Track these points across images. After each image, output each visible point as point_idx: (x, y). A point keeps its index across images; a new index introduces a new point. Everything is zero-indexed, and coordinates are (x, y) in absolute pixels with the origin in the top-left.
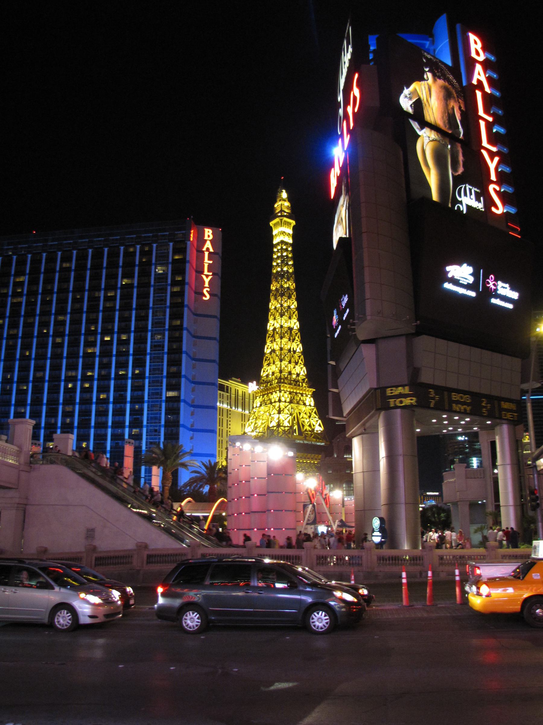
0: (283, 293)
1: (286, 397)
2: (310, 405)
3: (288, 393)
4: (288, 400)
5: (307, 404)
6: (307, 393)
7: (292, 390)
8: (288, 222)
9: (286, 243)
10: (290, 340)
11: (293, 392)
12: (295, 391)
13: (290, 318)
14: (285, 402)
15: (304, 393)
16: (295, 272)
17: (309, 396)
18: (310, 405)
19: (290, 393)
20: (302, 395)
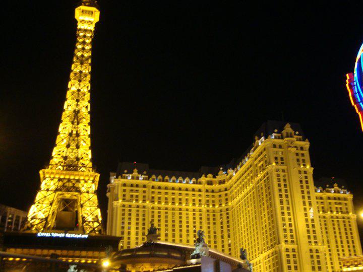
2: (88, 192)
3: (56, 180)
4: (53, 187)
5: (83, 189)
6: (87, 178)
7: (62, 177)
8: (89, 12)
10: (73, 123)
11: (64, 179)
12: (67, 177)
14: (48, 190)
15: (82, 178)
16: (92, 57)
17: (90, 182)
18: (88, 192)
19: (60, 180)
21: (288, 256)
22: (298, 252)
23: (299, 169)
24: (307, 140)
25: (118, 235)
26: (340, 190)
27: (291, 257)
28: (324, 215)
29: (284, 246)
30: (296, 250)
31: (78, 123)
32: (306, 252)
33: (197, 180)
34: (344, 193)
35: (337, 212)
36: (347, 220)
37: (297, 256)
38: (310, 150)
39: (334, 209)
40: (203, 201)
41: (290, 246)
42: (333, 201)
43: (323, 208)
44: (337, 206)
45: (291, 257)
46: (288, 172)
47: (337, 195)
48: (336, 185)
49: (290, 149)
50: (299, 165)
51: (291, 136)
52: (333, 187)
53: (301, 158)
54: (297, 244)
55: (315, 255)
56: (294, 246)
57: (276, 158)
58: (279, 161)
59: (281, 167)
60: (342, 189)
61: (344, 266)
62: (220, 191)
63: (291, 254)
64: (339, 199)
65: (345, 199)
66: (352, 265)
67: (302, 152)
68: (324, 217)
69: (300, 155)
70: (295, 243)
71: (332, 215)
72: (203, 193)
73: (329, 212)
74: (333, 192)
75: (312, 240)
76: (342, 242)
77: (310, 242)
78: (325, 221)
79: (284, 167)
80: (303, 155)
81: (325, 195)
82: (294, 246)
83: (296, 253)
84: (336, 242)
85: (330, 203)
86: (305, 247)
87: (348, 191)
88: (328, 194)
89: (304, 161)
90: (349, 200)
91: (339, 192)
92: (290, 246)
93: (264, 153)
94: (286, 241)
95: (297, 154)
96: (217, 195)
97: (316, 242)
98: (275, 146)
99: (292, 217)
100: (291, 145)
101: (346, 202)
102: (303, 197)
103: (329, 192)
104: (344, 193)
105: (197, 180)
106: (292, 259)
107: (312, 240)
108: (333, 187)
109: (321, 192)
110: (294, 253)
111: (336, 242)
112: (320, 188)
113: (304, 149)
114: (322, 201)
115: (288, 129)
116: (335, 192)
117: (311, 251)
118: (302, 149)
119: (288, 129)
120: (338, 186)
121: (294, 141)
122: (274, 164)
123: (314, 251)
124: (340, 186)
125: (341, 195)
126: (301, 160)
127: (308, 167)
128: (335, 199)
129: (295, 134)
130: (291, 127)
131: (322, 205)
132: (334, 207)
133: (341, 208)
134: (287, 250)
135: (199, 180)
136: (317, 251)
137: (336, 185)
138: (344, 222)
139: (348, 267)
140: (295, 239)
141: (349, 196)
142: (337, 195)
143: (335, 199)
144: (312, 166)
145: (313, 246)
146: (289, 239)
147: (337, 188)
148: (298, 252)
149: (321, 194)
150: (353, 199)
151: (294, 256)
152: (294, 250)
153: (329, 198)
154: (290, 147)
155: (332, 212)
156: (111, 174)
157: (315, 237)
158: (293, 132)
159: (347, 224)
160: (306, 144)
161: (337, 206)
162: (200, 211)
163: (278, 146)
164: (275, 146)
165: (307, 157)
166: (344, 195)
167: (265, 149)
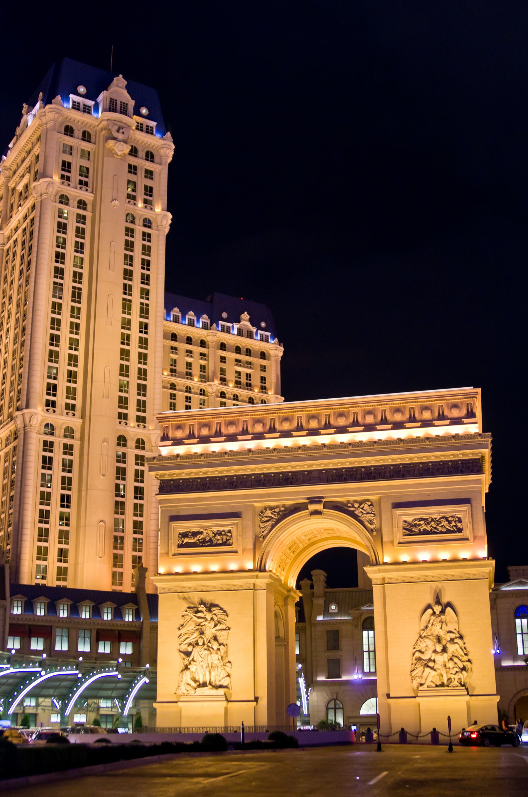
21: (48, 446)
22: (82, 439)
24: (169, 134)
26: (254, 330)
27: (58, 449)
28: (203, 386)
29: (38, 415)
30: (77, 435)
32: (105, 440)
34: (262, 340)
35: (238, 383)
37: (76, 451)
38: (174, 168)
39: (231, 376)
41: (61, 420)
42: (231, 356)
43: (203, 368)
44: (239, 369)
45: (58, 449)
46: (93, 211)
47: (244, 342)
48: (245, 316)
49: (111, 143)
50: (132, 198)
52: (239, 321)
53: (142, 181)
54: (83, 417)
56: (75, 422)
57: (66, 166)
58: (75, 175)
59: (76, 193)
60: (259, 328)
61: (165, 438)
63: (59, 441)
64: (248, 352)
65: (263, 355)
66: (191, 436)
67: (149, 166)
68: (202, 392)
69: (141, 173)
70: (78, 412)
71: (223, 388)
73: (217, 382)
74: (236, 332)
75: (132, 411)
77: (123, 417)
79: (87, 196)
80: (149, 174)
81: (215, 336)
82: (75, 422)
83: (76, 443)
85: (223, 359)
86: (103, 427)
87: (273, 337)
88: (224, 337)
89: (149, 191)
90: (273, 358)
91: (250, 335)
92: (61, 420)
93: (37, 150)
95: (132, 169)
97: (141, 420)
98: (69, 131)
99: (81, 337)
100: (116, 134)
101: (263, 362)
102: (127, 289)
103: (228, 331)
106: (58, 456)
107: (132, 411)
109: (205, 327)
110: (68, 441)
112: (205, 318)
113: (156, 159)
114: (204, 350)
115: (119, 88)
116: (240, 333)
117: (122, 441)
118: (150, 156)
120: (251, 321)
121: (129, 127)
122: (56, 179)
123: (131, 443)
124: (254, 322)
125: (256, 344)
126: (140, 189)
127: (159, 208)
128: (238, 350)
130: (128, 88)
131: (203, 362)
132: (231, 370)
133: (248, 376)
137: (245, 316)
139: (178, 442)
141: (275, 350)
143: (238, 350)
144: (169, 209)
145: (132, 430)
147: (248, 324)
148: (82, 439)
149: (205, 332)
150: (282, 357)
151: (68, 449)
152: (69, 432)
153: (223, 346)
154: (115, 139)
155: (223, 381)
157: (141, 405)
158: (131, 103)
160: (165, 147)
161: (239, 369)
163: (78, 133)
164: (69, 131)
165: (161, 184)
167: (39, 139)
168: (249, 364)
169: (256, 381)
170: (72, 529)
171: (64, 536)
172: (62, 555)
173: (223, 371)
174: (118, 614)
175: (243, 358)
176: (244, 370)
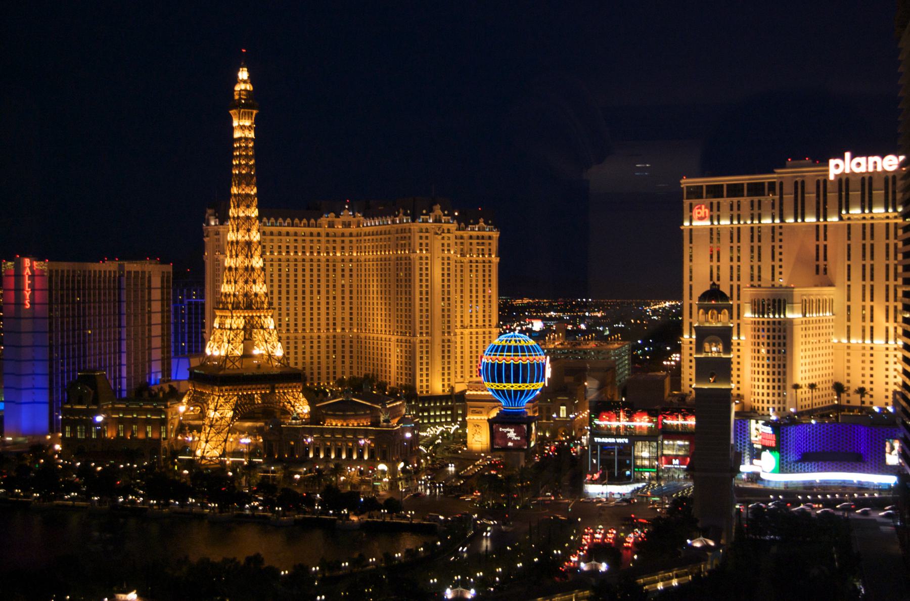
0: (243, 200)
1: (241, 323)
9: (246, 139)
10: (247, 256)
13: (249, 230)
19: (245, 317)
20: (260, 317)
21: (421, 347)
23: (443, 255)
25: (300, 367)
31: (252, 257)
33: (316, 221)
36: (487, 265)
39: (475, 251)
40: (323, 248)
41: (425, 338)
42: (474, 241)
43: (462, 250)
47: (481, 233)
48: (482, 220)
50: (443, 250)
51: (440, 221)
55: (446, 344)
56: (429, 338)
62: (343, 235)
64: (483, 238)
65: (490, 238)
72: (323, 239)
76: (477, 292)
78: (462, 266)
84: (471, 291)
91: (484, 230)
92: (425, 338)
94: (421, 333)
96: (338, 239)
104: (491, 230)
105: (316, 221)
108: (478, 223)
111: (471, 291)
116: (479, 230)
117: (443, 341)
119: (438, 210)
124: (486, 223)
128: (478, 238)
129: (445, 215)
134: (421, 342)
135: (319, 221)
136: (449, 341)
137: (482, 220)
138: (484, 266)
140: (429, 331)
141: (495, 234)
142: (481, 233)
143: (478, 238)
146: (424, 331)
151: (427, 347)
156: (209, 211)
159: (487, 269)
162: (319, 260)
166: (491, 233)
168: (483, 244)
169: (486, 251)
170: (429, 372)
171: (427, 375)
172: (427, 381)
173: (471, 250)
174: (447, 403)
175: (481, 241)
176: (480, 247)
